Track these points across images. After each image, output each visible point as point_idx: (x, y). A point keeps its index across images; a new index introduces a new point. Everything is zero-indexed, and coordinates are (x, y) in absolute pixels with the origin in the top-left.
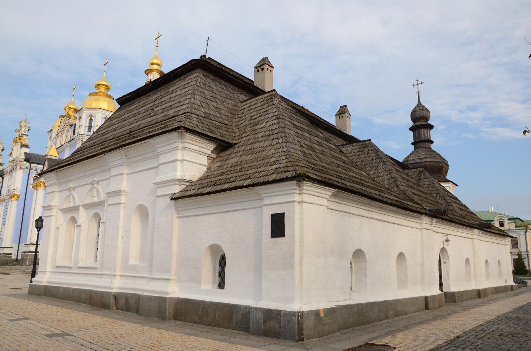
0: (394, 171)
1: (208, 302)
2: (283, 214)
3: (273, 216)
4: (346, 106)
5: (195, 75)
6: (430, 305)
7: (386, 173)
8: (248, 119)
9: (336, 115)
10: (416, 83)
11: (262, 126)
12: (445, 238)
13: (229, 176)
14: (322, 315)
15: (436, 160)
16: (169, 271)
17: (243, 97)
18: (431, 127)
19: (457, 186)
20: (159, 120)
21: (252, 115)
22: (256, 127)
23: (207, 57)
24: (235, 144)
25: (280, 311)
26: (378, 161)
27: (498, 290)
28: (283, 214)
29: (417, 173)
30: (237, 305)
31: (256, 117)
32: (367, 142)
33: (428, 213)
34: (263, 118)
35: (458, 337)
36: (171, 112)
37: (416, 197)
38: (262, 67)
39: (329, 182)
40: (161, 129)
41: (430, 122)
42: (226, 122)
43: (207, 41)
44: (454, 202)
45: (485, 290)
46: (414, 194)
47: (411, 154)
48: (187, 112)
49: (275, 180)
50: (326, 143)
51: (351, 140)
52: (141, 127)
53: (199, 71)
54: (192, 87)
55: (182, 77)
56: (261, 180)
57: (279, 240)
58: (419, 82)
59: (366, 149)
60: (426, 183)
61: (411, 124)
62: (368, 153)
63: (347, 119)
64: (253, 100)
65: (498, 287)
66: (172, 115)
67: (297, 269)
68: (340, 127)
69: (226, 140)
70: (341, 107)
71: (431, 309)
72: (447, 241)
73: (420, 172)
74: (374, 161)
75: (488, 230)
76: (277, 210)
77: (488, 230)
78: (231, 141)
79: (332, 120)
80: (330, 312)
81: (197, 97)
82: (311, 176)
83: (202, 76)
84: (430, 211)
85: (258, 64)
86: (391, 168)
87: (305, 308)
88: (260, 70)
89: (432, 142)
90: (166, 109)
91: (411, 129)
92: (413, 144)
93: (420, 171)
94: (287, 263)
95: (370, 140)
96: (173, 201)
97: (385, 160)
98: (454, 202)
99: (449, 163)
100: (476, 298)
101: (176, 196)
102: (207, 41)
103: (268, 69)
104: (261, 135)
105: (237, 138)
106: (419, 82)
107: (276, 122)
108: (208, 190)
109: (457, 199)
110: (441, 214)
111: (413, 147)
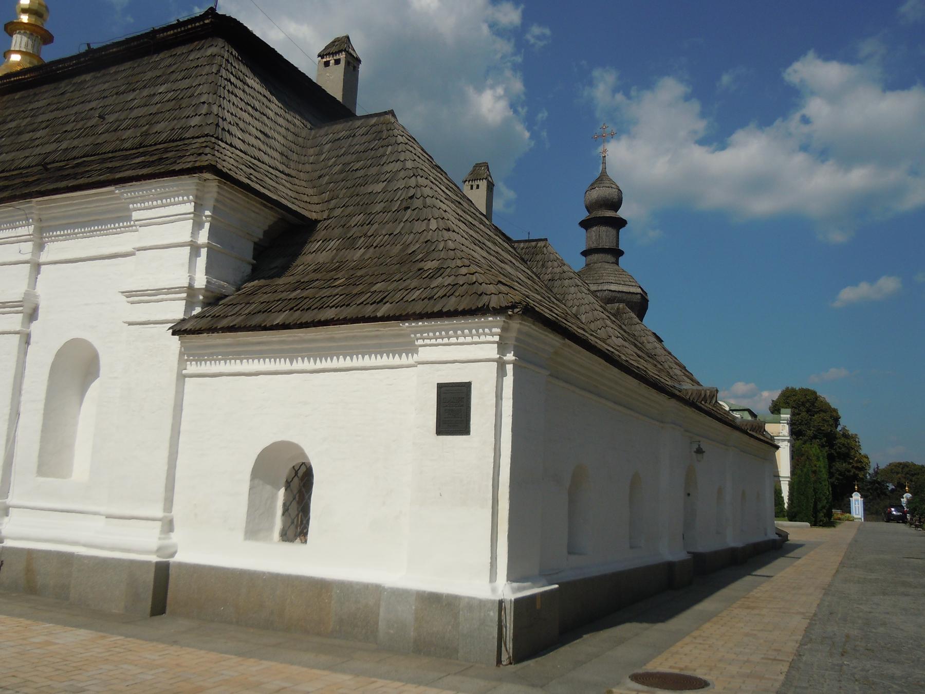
2: (467, 386)
3: (441, 387)
8: (337, 168)
12: (695, 447)
13: (326, 292)
18: (620, 223)
22: (362, 190)
24: (317, 222)
26: (567, 282)
28: (467, 386)
32: (541, 244)
34: (373, 170)
36: (158, 127)
38: (337, 57)
40: (144, 165)
41: (622, 213)
42: (287, 171)
48: (207, 135)
52: (75, 153)
53: (220, 42)
54: (211, 78)
55: (179, 50)
59: (539, 257)
61: (585, 215)
62: (543, 266)
66: (163, 136)
72: (699, 451)
85: (327, 48)
88: (332, 62)
89: (621, 253)
90: (143, 121)
95: (546, 240)
96: (177, 337)
101: (188, 326)
104: (379, 207)
107: (412, 182)
108: (279, 319)
109: (684, 368)
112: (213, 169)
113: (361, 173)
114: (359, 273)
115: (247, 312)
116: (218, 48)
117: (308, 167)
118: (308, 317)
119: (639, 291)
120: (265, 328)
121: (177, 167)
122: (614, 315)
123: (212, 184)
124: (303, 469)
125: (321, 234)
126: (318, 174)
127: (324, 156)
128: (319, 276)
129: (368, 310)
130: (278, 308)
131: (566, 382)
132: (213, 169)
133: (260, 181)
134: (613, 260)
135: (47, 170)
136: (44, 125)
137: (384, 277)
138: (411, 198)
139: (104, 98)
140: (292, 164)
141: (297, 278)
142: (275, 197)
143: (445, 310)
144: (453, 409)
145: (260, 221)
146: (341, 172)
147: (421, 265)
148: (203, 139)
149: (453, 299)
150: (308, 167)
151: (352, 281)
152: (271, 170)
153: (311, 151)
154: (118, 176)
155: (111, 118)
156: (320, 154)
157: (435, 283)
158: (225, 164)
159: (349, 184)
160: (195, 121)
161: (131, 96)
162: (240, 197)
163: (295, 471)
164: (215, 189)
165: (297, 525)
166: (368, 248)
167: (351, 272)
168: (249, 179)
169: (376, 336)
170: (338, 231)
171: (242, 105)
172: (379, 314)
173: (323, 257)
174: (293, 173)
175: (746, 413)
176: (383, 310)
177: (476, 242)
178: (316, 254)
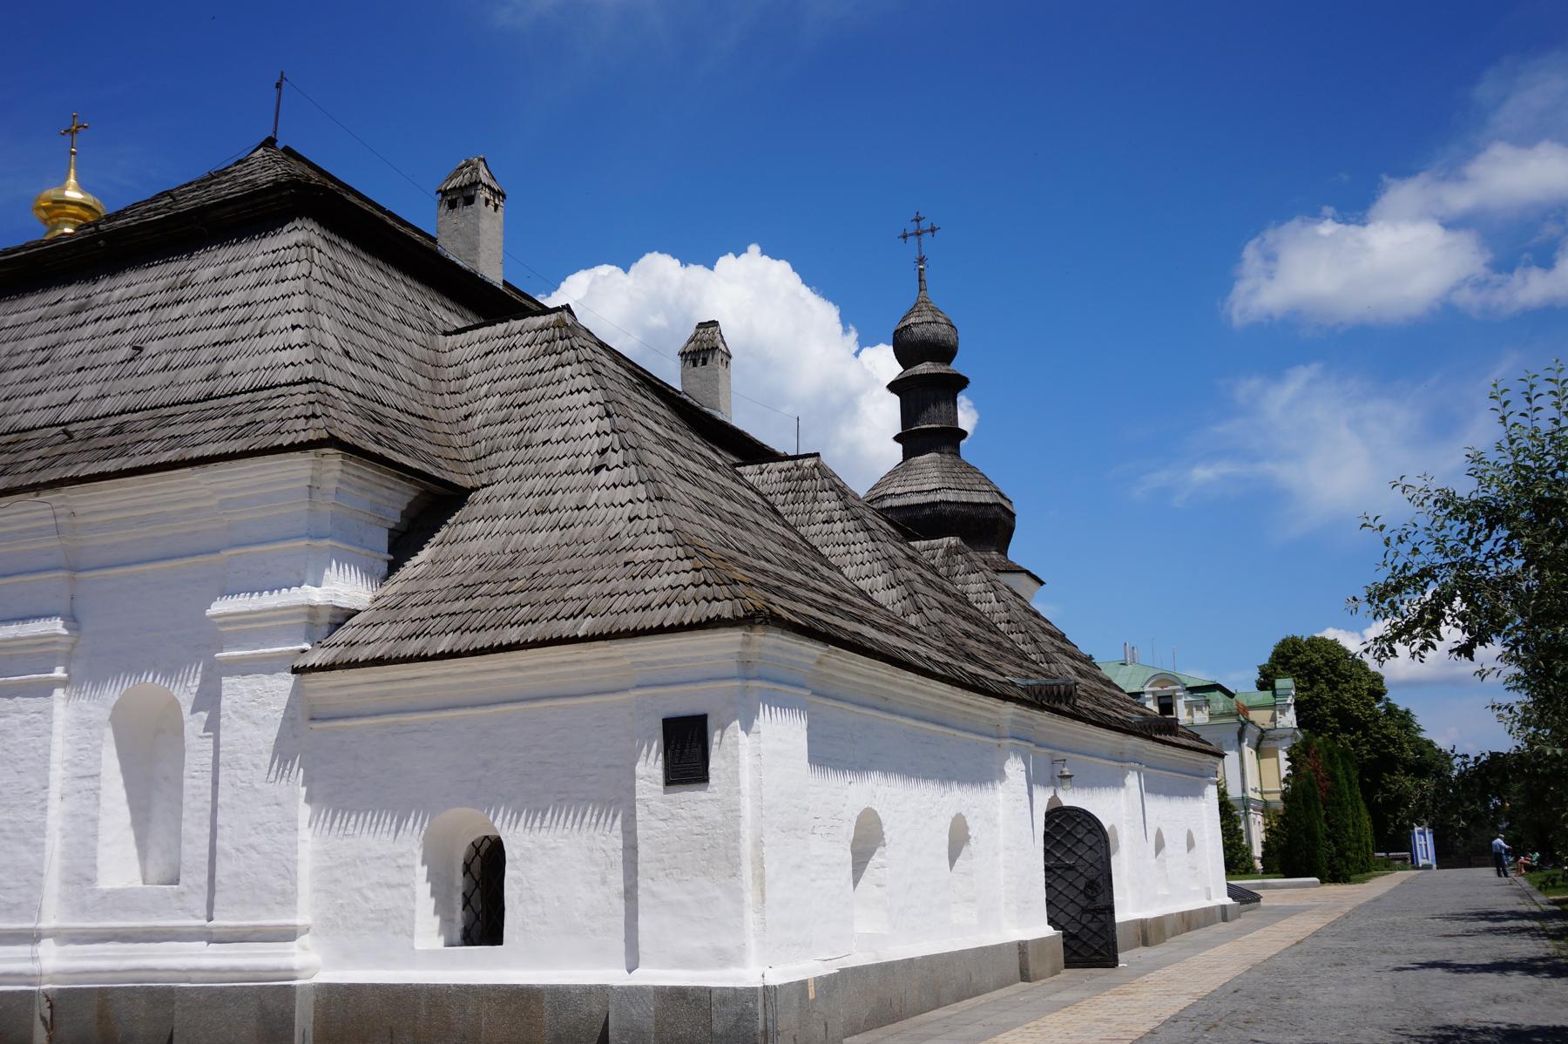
0: (902, 562)
1: (448, 986)
3: (664, 720)
4: (714, 323)
5: (299, 236)
6: (1033, 967)
7: (877, 565)
8: (494, 401)
9: (682, 354)
10: (912, 228)
14: (812, 996)
16: (288, 899)
19: (1042, 583)
20: (190, 392)
21: (502, 386)
23: (280, 145)
25: (710, 990)
27: (1189, 922)
29: (941, 552)
30: (567, 987)
31: (522, 397)
32: (809, 462)
33: (1025, 696)
35: (1153, 1032)
37: (972, 643)
39: (822, 628)
41: (957, 366)
43: (278, 86)
44: (1060, 650)
45: (1159, 921)
46: (968, 635)
47: (893, 473)
48: (307, 381)
49: (681, 624)
50: (734, 486)
51: (750, 451)
52: (106, 406)
54: (301, 284)
56: (633, 621)
57: (688, 796)
58: (925, 225)
60: (973, 588)
61: (894, 370)
62: (815, 499)
63: (722, 368)
64: (486, 331)
65: (1190, 912)
66: (245, 381)
67: (747, 870)
68: (698, 397)
69: (448, 477)
70: (701, 325)
71: (1037, 979)
73: (950, 552)
74: (838, 526)
75: (1168, 738)
77: (1168, 738)
78: (457, 479)
79: (670, 373)
80: (828, 984)
81: (326, 322)
82: (785, 614)
83: (319, 242)
84: (1026, 689)
86: (892, 550)
87: (777, 977)
90: (205, 355)
91: (893, 387)
92: (897, 438)
93: (949, 547)
94: (718, 855)
95: (817, 455)
98: (1060, 650)
99: (1015, 509)
100: (1136, 946)
102: (278, 86)
103: (487, 201)
104: (563, 465)
105: (471, 467)
106: (925, 225)
108: (444, 644)
109: (1063, 638)
110: (1059, 698)
111: (898, 448)
112: (333, 442)
113: (531, 409)
114: (545, 570)
115: (395, 634)
116: (300, 233)
118: (484, 639)
120: (426, 658)
121: (286, 440)
122: (933, 569)
123: (333, 460)
124: (487, 844)
125: (478, 505)
126: (464, 411)
127: (470, 380)
129: (566, 628)
130: (438, 629)
131: (837, 699)
132: (333, 442)
133: (393, 443)
135: (70, 435)
136: (41, 355)
137: (578, 576)
138: (604, 451)
139: (134, 312)
143: (666, 624)
145: (396, 499)
146: (500, 408)
147: (630, 555)
148: (305, 388)
149: (675, 607)
151: (536, 582)
152: (404, 418)
154: (197, 452)
155: (152, 347)
157: (649, 584)
158: (344, 427)
159: (515, 427)
160: (286, 356)
161: (180, 310)
162: (368, 472)
163: (475, 847)
164: (339, 467)
165: (483, 919)
167: (534, 568)
168: (378, 442)
171: (351, 319)
172: (580, 634)
174: (431, 412)
175: (1218, 694)
176: (585, 626)
177: (705, 509)
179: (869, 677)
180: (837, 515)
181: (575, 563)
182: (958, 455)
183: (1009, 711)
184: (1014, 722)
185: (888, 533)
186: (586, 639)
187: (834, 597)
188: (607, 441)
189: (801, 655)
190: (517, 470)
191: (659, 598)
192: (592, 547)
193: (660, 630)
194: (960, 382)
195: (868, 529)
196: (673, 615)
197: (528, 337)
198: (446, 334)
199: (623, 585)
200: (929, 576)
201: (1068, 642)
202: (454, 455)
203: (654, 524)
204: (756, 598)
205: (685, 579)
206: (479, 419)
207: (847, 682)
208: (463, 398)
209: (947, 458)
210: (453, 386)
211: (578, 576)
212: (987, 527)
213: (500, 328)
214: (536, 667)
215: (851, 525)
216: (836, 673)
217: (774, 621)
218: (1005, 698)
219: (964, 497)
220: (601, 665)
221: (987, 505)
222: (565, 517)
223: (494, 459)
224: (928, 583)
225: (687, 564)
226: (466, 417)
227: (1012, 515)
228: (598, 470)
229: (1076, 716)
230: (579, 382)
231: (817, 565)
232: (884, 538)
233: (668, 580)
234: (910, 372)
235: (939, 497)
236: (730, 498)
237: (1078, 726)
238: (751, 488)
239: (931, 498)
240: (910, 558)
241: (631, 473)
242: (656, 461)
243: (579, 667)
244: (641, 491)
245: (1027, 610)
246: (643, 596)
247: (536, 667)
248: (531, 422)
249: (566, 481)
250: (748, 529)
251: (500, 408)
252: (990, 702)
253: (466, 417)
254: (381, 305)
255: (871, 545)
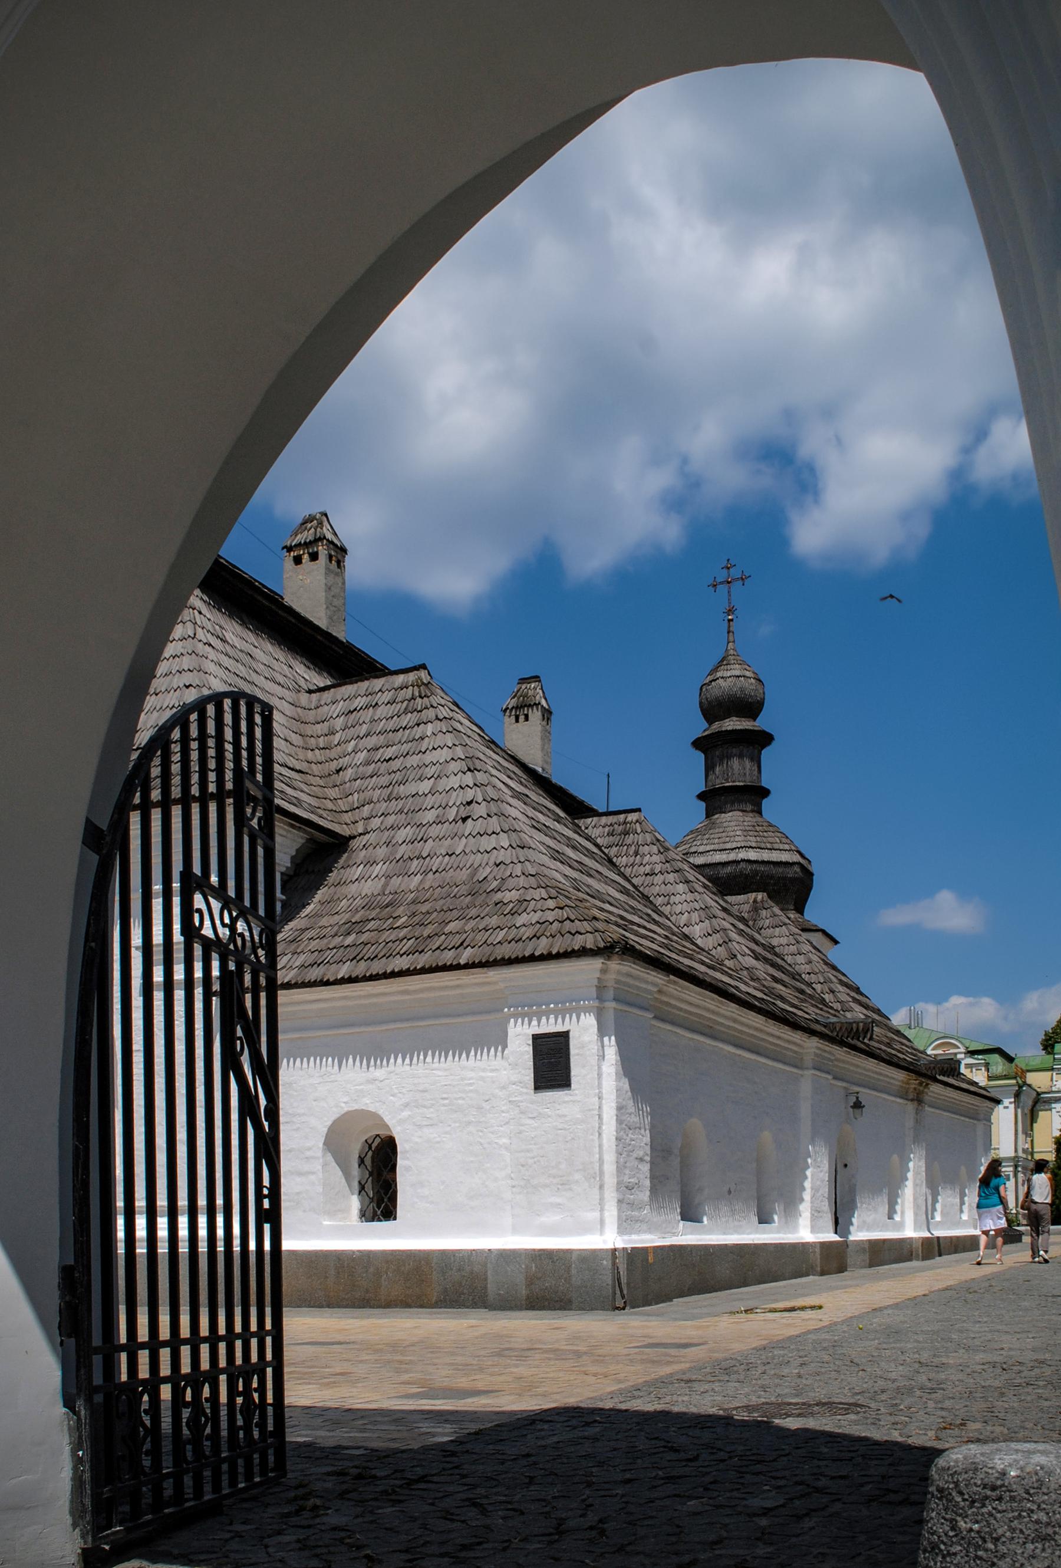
2: (565, 1036)
3: (536, 1038)
7: (695, 916)
8: (362, 756)
11: (425, 786)
14: (651, 1259)
15: (775, 856)
17: (321, 680)
19: (836, 942)
22: (402, 790)
28: (565, 1036)
31: (389, 752)
34: (414, 760)
41: (760, 723)
50: (576, 837)
62: (636, 853)
64: (348, 690)
74: (659, 879)
76: (550, 1026)
89: (765, 793)
92: (701, 796)
95: (639, 810)
97: (692, 878)
99: (814, 868)
104: (430, 816)
105: (347, 818)
110: (857, 1035)
113: (396, 765)
114: (424, 908)
117: (319, 755)
119: (796, 858)
122: (742, 919)
126: (334, 765)
127: (338, 736)
128: (373, 914)
129: (448, 957)
131: (673, 1023)
134: (749, 807)
137: (455, 914)
138: (469, 803)
140: (301, 754)
141: (346, 917)
142: (305, 815)
143: (537, 954)
144: (552, 1064)
146: (368, 763)
147: (499, 896)
149: (543, 939)
150: (319, 755)
151: (416, 919)
153: (319, 729)
156: (333, 733)
157: (520, 920)
159: (384, 780)
166: (426, 873)
169: (458, 986)
170: (381, 852)
172: (462, 962)
173: (369, 887)
177: (557, 856)
178: (357, 882)
179: (697, 1006)
180: (657, 869)
181: (449, 903)
182: (759, 812)
183: (812, 1045)
184: (816, 1055)
185: (705, 886)
186: (467, 966)
187: (667, 937)
188: (469, 794)
189: (647, 982)
190: (391, 820)
191: (529, 932)
192: (464, 889)
193: (532, 959)
194: (764, 739)
195: (687, 882)
196: (542, 946)
197: (387, 696)
198: (310, 692)
199: (494, 921)
200: (741, 926)
201: (862, 994)
202: (330, 805)
203: (518, 869)
204: (615, 933)
205: (550, 916)
206: (349, 773)
207: (681, 1009)
208: (333, 754)
209: (750, 819)
210: (321, 742)
211: (455, 914)
212: (791, 886)
213: (364, 686)
214: (422, 991)
215: (671, 877)
216: (673, 1002)
217: (629, 952)
218: (812, 1033)
219: (766, 856)
220: (478, 989)
221: (787, 864)
222: (435, 863)
223: (366, 811)
224: (741, 933)
225: (551, 903)
226: (338, 771)
227: (812, 874)
228: (464, 820)
229: (870, 1054)
230: (440, 740)
231: (650, 912)
232: (701, 890)
233: (535, 917)
234: (716, 727)
235: (742, 855)
236: (574, 848)
237: (871, 1064)
238: (588, 838)
239: (732, 856)
240: (724, 910)
241: (494, 824)
242: (514, 813)
243: (458, 991)
244: (504, 840)
245: (826, 963)
246: (514, 931)
247: (422, 991)
248: (398, 776)
249: (435, 831)
250: (591, 876)
251: (368, 763)
252: (797, 1036)
253: (338, 771)
254: (254, 665)
255: (690, 897)
